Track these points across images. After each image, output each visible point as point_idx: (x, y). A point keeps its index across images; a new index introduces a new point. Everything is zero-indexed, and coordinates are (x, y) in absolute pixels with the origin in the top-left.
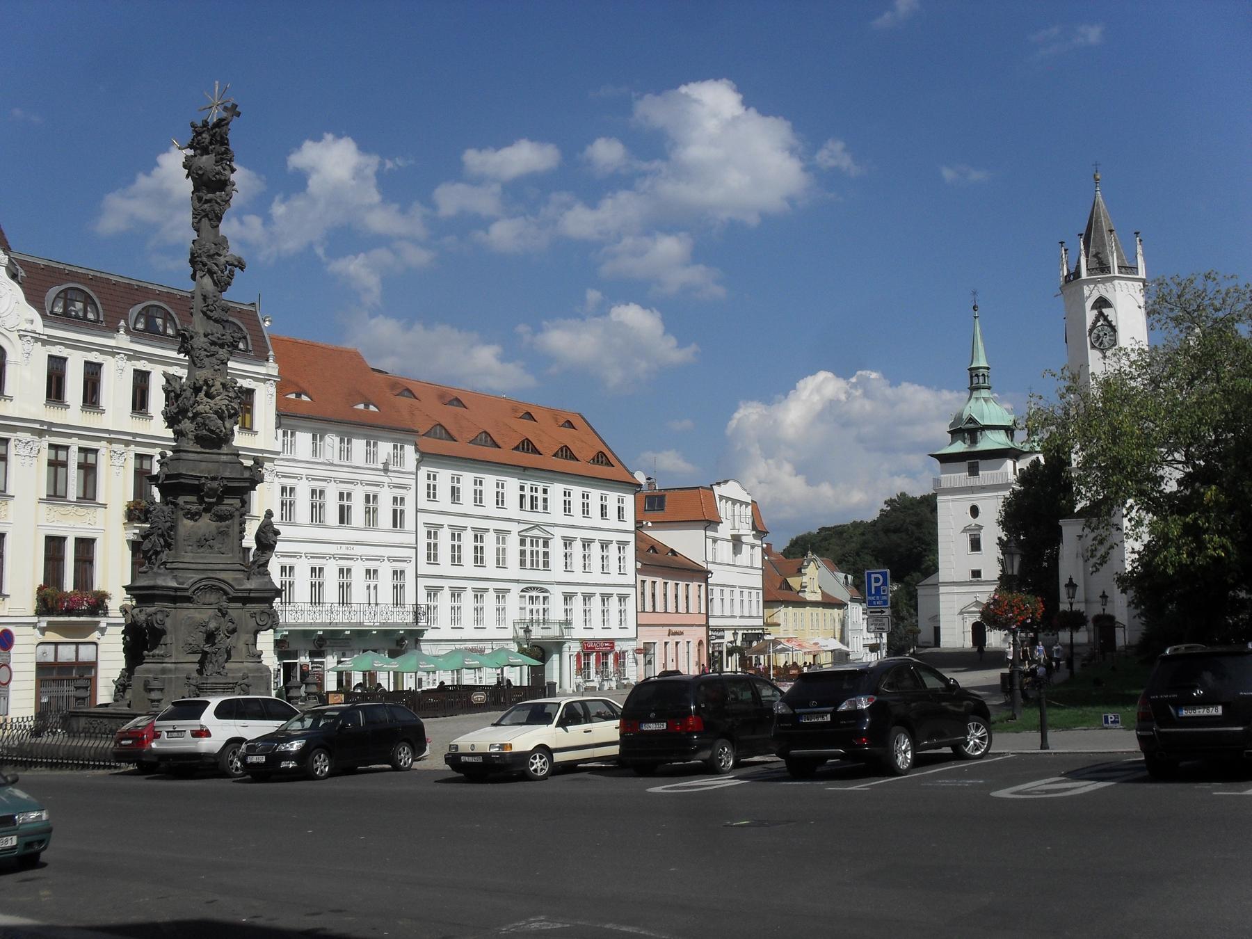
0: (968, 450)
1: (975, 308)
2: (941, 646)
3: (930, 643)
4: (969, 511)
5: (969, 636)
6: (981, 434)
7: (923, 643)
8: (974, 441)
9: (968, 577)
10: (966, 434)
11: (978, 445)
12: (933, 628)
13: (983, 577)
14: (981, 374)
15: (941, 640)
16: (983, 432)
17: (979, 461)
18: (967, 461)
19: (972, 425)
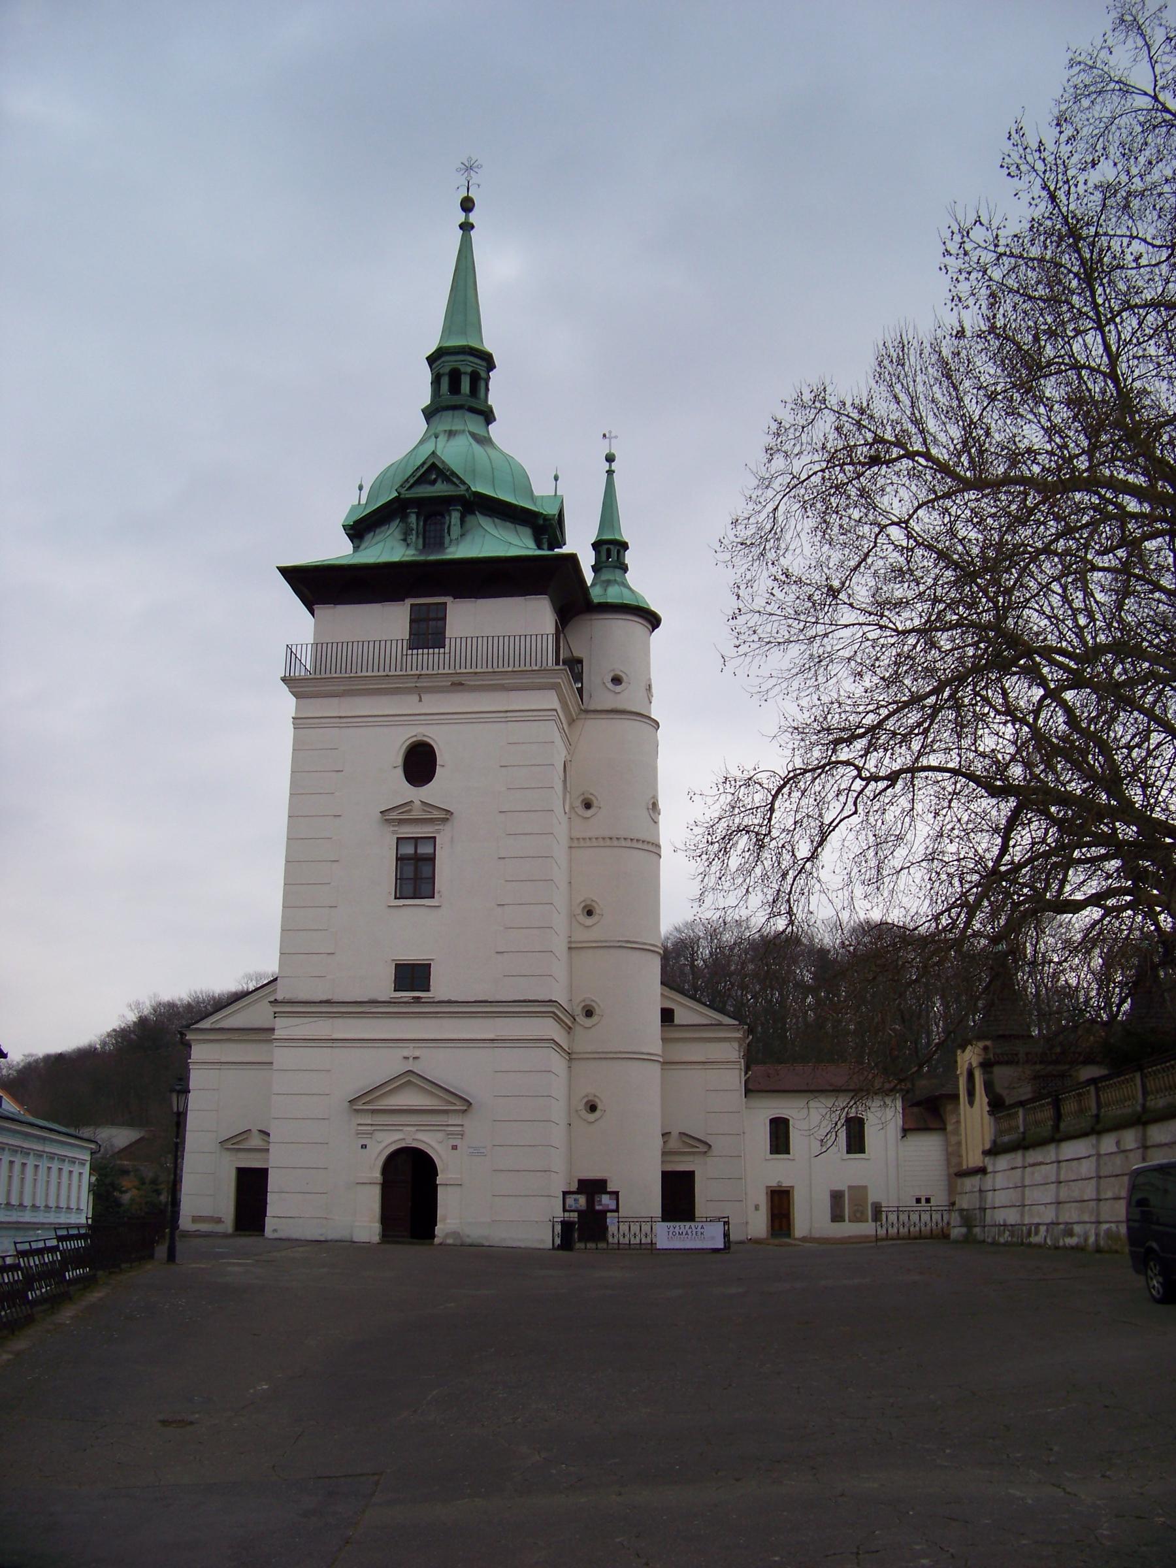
0: (422, 558)
1: (467, 205)
2: (268, 1232)
3: (219, 1221)
4: (400, 761)
5: (370, 1201)
6: (462, 521)
7: (196, 1219)
8: (434, 538)
9: (383, 985)
10: (413, 519)
11: (451, 549)
12: (233, 1175)
13: (441, 986)
14: (469, 370)
15: (271, 1210)
16: (470, 519)
17: (448, 600)
18: (409, 602)
19: (441, 489)
